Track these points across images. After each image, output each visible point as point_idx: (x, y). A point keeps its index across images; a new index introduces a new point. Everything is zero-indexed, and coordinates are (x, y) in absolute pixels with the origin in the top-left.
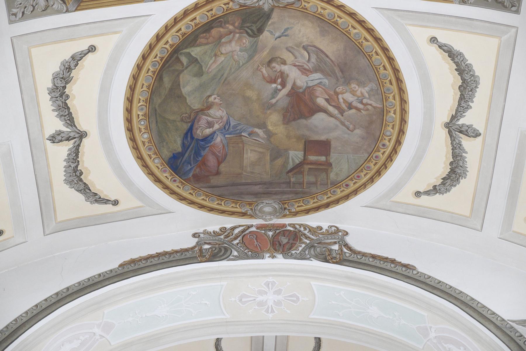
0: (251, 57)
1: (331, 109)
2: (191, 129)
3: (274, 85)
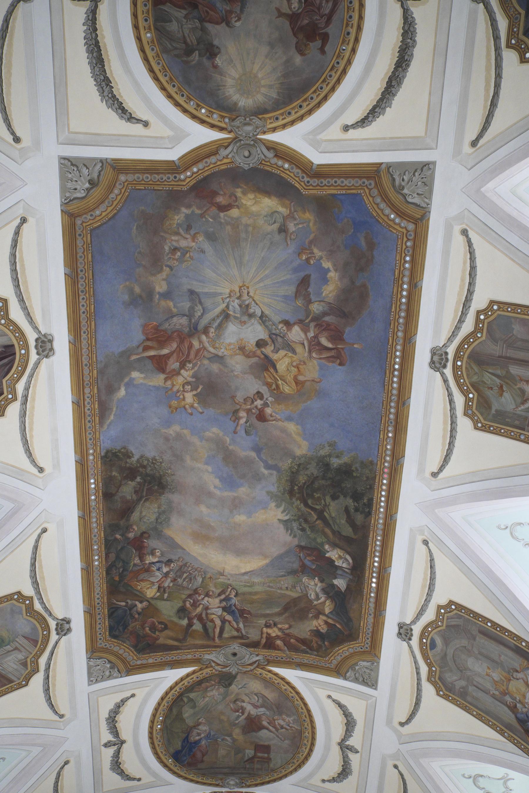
0: (224, 698)
1: (271, 728)
2: (187, 737)
3: (237, 713)
